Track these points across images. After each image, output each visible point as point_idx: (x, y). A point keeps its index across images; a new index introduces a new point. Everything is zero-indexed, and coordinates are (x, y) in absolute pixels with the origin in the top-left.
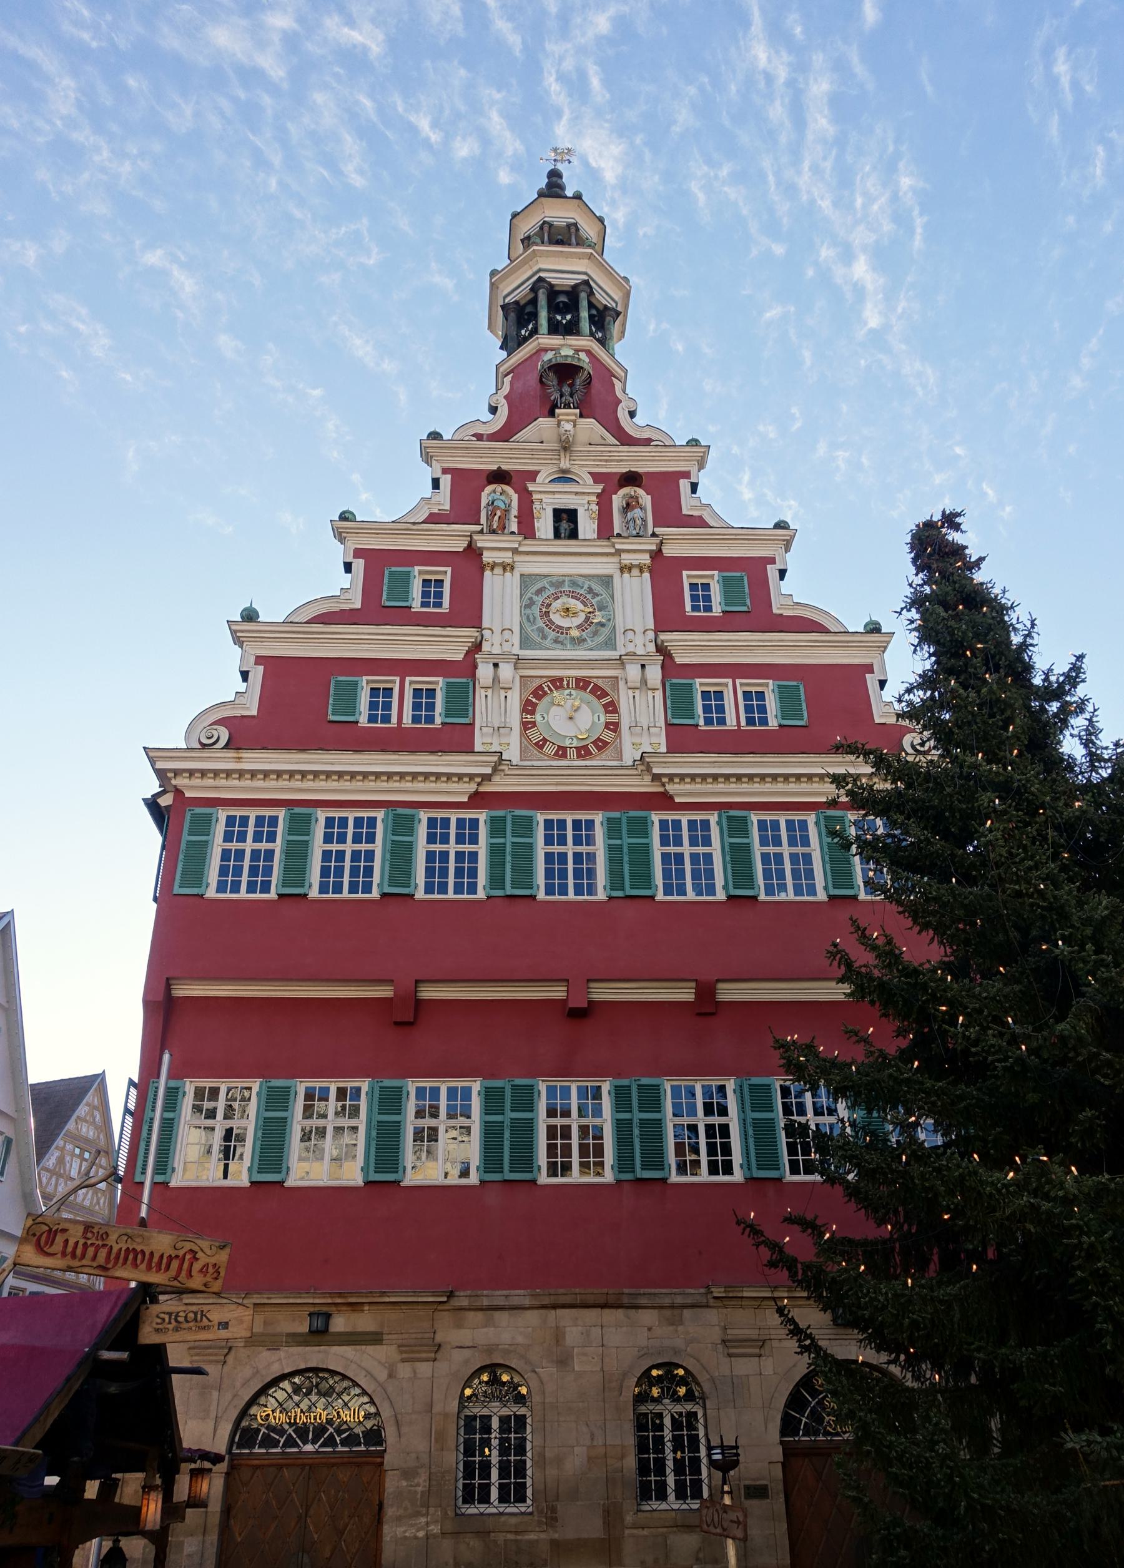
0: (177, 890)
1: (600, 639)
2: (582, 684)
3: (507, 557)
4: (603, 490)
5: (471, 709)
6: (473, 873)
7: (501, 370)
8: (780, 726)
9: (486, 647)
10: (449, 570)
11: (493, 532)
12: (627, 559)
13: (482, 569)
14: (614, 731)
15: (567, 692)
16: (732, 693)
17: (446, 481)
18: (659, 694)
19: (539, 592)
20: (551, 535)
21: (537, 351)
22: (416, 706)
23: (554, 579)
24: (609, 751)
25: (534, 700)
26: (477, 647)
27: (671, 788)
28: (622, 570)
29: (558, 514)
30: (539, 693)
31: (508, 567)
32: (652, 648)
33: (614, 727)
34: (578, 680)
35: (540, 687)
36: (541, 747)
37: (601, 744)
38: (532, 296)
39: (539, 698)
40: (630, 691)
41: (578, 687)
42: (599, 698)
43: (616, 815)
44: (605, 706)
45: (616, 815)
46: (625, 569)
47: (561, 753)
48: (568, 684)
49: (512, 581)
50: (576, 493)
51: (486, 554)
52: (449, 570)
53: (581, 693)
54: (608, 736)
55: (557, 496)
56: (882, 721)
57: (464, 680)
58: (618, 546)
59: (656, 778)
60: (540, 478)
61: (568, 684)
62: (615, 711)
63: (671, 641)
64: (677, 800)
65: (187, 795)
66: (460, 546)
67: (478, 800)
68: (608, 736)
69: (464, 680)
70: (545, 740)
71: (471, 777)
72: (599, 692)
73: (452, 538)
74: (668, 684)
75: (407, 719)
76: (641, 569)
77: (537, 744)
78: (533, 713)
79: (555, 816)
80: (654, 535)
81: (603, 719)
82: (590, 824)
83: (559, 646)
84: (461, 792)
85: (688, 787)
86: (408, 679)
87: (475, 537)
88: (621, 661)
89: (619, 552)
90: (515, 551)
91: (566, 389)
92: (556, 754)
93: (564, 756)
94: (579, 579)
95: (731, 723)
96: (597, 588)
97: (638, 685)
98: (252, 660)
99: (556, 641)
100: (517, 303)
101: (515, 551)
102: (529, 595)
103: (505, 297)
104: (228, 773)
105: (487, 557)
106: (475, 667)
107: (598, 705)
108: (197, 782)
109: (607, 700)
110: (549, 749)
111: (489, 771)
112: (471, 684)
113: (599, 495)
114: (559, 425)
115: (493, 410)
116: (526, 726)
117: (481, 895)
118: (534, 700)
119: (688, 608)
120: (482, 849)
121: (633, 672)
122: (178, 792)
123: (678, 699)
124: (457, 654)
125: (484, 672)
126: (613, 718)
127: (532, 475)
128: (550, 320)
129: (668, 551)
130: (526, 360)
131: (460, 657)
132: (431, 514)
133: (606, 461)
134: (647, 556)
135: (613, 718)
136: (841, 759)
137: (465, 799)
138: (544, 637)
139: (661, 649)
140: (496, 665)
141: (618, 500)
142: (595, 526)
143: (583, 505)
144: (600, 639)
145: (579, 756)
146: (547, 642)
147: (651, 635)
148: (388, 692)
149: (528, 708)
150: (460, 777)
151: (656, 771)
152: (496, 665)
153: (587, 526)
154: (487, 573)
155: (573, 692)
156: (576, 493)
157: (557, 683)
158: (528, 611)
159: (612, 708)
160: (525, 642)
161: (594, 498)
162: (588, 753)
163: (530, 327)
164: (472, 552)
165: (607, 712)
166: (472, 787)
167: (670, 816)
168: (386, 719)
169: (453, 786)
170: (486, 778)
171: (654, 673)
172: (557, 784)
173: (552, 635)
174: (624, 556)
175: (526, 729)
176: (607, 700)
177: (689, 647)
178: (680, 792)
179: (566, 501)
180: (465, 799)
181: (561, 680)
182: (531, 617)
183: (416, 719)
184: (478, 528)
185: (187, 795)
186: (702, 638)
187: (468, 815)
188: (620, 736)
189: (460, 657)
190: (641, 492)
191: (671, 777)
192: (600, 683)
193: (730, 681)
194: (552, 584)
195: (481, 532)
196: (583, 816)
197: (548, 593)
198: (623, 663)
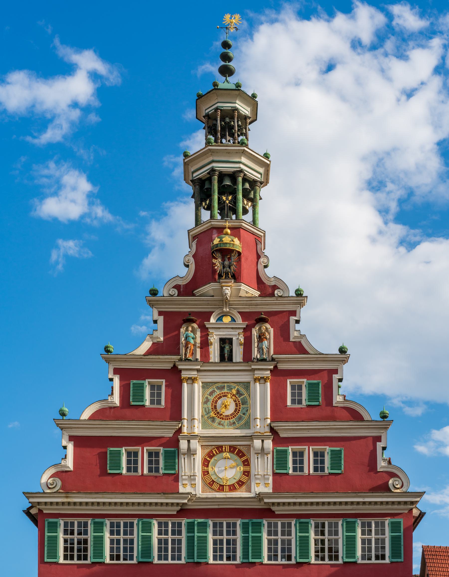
0: (46, 560)
1: (243, 422)
2: (232, 449)
3: (194, 374)
4: (247, 326)
5: (177, 466)
6: (180, 550)
7: (191, 233)
8: (329, 473)
10: (164, 381)
11: (187, 360)
12: (258, 374)
13: (181, 382)
14: (247, 476)
16: (309, 453)
17: (161, 319)
18: (270, 456)
19: (211, 394)
20: (217, 360)
21: (211, 228)
22: (150, 462)
23: (219, 385)
24: (244, 487)
25: (208, 459)
26: (179, 430)
27: (274, 508)
29: (223, 341)
30: (211, 455)
32: (267, 429)
33: (247, 473)
34: (231, 447)
35: (212, 451)
36: (212, 485)
37: (241, 483)
38: (208, 176)
40: (256, 455)
41: (230, 451)
42: (241, 457)
43: (246, 521)
44: (244, 462)
45: (246, 521)
47: (221, 488)
48: (225, 450)
49: (197, 386)
50: (232, 328)
51: (183, 372)
52: (164, 381)
53: (232, 455)
54: (244, 479)
55: (221, 330)
56: (381, 470)
57: (173, 449)
58: (253, 367)
59: (265, 503)
60: (213, 320)
61: (225, 450)
62: (248, 465)
63: (277, 426)
64: (276, 513)
66: (169, 366)
68: (244, 479)
69: (173, 449)
70: (213, 481)
71: (178, 504)
72: (240, 454)
73: (164, 362)
74: (275, 450)
75: (146, 471)
77: (209, 483)
78: (207, 466)
79: (218, 520)
80: (273, 360)
81: (242, 469)
82: (235, 525)
83: (221, 427)
84: (173, 511)
85: (281, 508)
86: (145, 448)
87: (177, 364)
88: (251, 438)
89: (254, 370)
91: (227, 263)
92: (219, 489)
93: (223, 490)
94: (233, 384)
95: (306, 471)
96: (242, 390)
97: (260, 452)
98: (67, 438)
99: (219, 424)
100: (200, 179)
101: (198, 370)
102: (206, 396)
103: (193, 173)
104: (63, 503)
105: (184, 375)
106: (178, 441)
107: (240, 461)
108: (49, 507)
109: (244, 458)
110: (215, 486)
111: (186, 501)
112: (177, 451)
113: (244, 329)
114: (222, 287)
115: (187, 266)
116: (205, 473)
117: (183, 561)
118: (208, 459)
119: (289, 403)
120: (184, 537)
121: (257, 443)
122: (40, 511)
123: (280, 460)
124: (169, 434)
125: (183, 444)
126: (247, 469)
127: (207, 316)
128: (219, 199)
129: (281, 366)
130: (205, 232)
132: (153, 343)
133: (249, 305)
134: (269, 372)
135: (247, 469)
136: (355, 495)
139: (272, 430)
140: (189, 441)
141: (255, 332)
143: (235, 335)
144: (243, 422)
145: (230, 490)
146: (216, 424)
147: (269, 421)
148: (136, 454)
149: (206, 463)
150: (172, 504)
151: (266, 500)
152: (189, 441)
153: (238, 354)
156: (232, 328)
157: (220, 449)
158: (205, 406)
159: (247, 463)
160: (205, 426)
161: (241, 331)
163: (208, 202)
164: (175, 372)
165: (244, 465)
166: (179, 508)
167: (273, 520)
168: (136, 470)
169: (170, 508)
170: (184, 504)
171: (269, 444)
172: (219, 505)
173: (218, 420)
174: (256, 372)
175: (204, 475)
176: (244, 458)
177: (287, 429)
178: (277, 510)
179: (225, 334)
180: (175, 513)
181: (221, 447)
182: (207, 409)
183: (150, 470)
184: (179, 357)
185: (45, 512)
186: (293, 425)
187: (176, 520)
188: (250, 478)
189: (171, 435)
190: (268, 326)
191: (273, 504)
192: (241, 448)
193: (307, 447)
194: (218, 388)
195: (181, 360)
196: (231, 520)
197: (216, 394)
198: (252, 439)
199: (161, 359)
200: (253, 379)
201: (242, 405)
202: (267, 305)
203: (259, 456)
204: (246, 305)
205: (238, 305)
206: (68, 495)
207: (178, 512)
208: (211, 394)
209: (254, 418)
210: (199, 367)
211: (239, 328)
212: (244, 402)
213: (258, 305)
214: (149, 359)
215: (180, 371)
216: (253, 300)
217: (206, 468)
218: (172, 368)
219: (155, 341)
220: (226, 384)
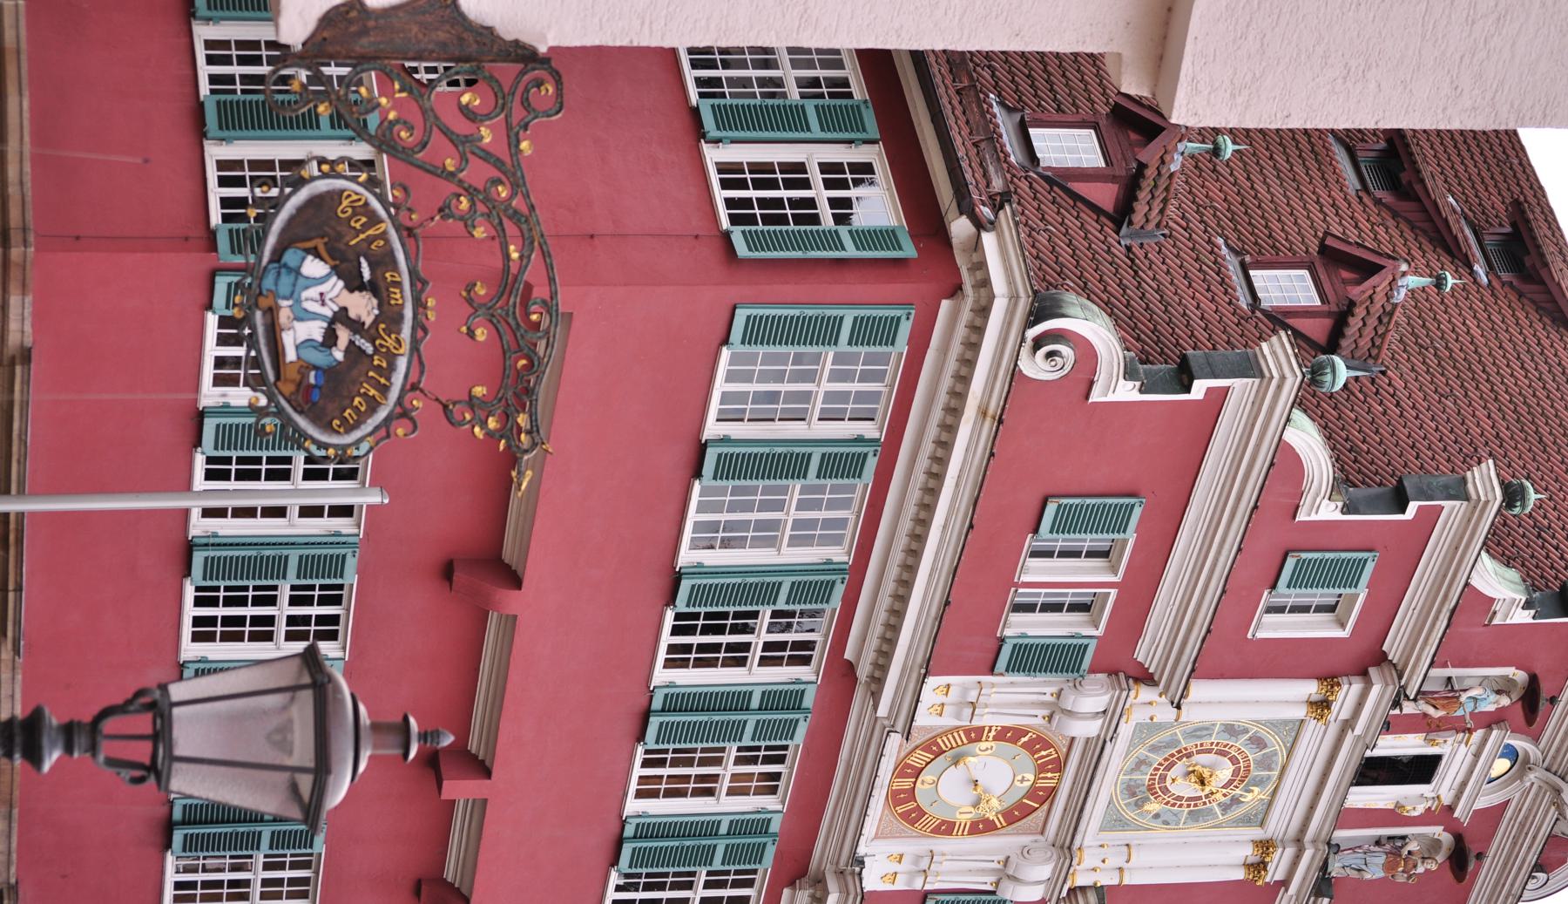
9: (1146, 693)
15: (1031, 777)
28: (1265, 846)
31: (1321, 706)
33: (946, 829)
34: (1052, 792)
37: (914, 817)
39: (1029, 747)
46: (1265, 846)
50: (1464, 784)
51: (1357, 686)
52: (1344, 634)
65: (945, 304)
66: (1394, 646)
67: (842, 675)
76: (1259, 866)
83: (1130, 763)
90: (1348, 725)
116: (975, 735)
131: (1140, 655)
133: (1522, 825)
137: (848, 654)
138: (1154, 749)
142: (1381, 805)
154: (1311, 688)
155: (1027, 784)
156: (1464, 784)
162: (897, 802)
166: (863, 672)
174: (1290, 852)
180: (848, 654)
185: (945, 304)
189: (1140, 655)
199: (1422, 649)
200: (1268, 835)
201: (1190, 813)
202: (1505, 864)
203: (1000, 866)
204: (1526, 818)
205: (1534, 800)
206: (988, 421)
207: (850, 668)
208: (1258, 742)
209: (1133, 843)
210: (1359, 729)
211: (1458, 797)
212: (1194, 816)
213: (1514, 843)
214: (1436, 618)
215: (1364, 674)
216: (1530, 848)
217: (993, 733)
218: (1385, 655)
219: (1496, 607)
220: (1276, 773)
